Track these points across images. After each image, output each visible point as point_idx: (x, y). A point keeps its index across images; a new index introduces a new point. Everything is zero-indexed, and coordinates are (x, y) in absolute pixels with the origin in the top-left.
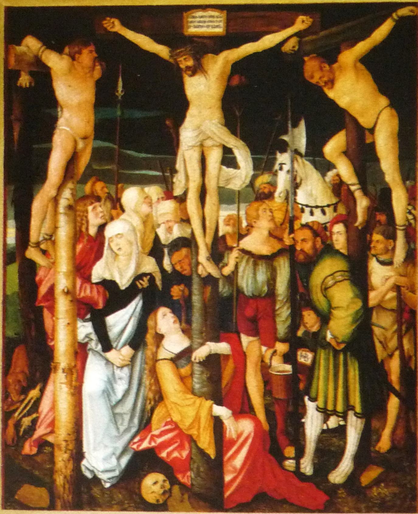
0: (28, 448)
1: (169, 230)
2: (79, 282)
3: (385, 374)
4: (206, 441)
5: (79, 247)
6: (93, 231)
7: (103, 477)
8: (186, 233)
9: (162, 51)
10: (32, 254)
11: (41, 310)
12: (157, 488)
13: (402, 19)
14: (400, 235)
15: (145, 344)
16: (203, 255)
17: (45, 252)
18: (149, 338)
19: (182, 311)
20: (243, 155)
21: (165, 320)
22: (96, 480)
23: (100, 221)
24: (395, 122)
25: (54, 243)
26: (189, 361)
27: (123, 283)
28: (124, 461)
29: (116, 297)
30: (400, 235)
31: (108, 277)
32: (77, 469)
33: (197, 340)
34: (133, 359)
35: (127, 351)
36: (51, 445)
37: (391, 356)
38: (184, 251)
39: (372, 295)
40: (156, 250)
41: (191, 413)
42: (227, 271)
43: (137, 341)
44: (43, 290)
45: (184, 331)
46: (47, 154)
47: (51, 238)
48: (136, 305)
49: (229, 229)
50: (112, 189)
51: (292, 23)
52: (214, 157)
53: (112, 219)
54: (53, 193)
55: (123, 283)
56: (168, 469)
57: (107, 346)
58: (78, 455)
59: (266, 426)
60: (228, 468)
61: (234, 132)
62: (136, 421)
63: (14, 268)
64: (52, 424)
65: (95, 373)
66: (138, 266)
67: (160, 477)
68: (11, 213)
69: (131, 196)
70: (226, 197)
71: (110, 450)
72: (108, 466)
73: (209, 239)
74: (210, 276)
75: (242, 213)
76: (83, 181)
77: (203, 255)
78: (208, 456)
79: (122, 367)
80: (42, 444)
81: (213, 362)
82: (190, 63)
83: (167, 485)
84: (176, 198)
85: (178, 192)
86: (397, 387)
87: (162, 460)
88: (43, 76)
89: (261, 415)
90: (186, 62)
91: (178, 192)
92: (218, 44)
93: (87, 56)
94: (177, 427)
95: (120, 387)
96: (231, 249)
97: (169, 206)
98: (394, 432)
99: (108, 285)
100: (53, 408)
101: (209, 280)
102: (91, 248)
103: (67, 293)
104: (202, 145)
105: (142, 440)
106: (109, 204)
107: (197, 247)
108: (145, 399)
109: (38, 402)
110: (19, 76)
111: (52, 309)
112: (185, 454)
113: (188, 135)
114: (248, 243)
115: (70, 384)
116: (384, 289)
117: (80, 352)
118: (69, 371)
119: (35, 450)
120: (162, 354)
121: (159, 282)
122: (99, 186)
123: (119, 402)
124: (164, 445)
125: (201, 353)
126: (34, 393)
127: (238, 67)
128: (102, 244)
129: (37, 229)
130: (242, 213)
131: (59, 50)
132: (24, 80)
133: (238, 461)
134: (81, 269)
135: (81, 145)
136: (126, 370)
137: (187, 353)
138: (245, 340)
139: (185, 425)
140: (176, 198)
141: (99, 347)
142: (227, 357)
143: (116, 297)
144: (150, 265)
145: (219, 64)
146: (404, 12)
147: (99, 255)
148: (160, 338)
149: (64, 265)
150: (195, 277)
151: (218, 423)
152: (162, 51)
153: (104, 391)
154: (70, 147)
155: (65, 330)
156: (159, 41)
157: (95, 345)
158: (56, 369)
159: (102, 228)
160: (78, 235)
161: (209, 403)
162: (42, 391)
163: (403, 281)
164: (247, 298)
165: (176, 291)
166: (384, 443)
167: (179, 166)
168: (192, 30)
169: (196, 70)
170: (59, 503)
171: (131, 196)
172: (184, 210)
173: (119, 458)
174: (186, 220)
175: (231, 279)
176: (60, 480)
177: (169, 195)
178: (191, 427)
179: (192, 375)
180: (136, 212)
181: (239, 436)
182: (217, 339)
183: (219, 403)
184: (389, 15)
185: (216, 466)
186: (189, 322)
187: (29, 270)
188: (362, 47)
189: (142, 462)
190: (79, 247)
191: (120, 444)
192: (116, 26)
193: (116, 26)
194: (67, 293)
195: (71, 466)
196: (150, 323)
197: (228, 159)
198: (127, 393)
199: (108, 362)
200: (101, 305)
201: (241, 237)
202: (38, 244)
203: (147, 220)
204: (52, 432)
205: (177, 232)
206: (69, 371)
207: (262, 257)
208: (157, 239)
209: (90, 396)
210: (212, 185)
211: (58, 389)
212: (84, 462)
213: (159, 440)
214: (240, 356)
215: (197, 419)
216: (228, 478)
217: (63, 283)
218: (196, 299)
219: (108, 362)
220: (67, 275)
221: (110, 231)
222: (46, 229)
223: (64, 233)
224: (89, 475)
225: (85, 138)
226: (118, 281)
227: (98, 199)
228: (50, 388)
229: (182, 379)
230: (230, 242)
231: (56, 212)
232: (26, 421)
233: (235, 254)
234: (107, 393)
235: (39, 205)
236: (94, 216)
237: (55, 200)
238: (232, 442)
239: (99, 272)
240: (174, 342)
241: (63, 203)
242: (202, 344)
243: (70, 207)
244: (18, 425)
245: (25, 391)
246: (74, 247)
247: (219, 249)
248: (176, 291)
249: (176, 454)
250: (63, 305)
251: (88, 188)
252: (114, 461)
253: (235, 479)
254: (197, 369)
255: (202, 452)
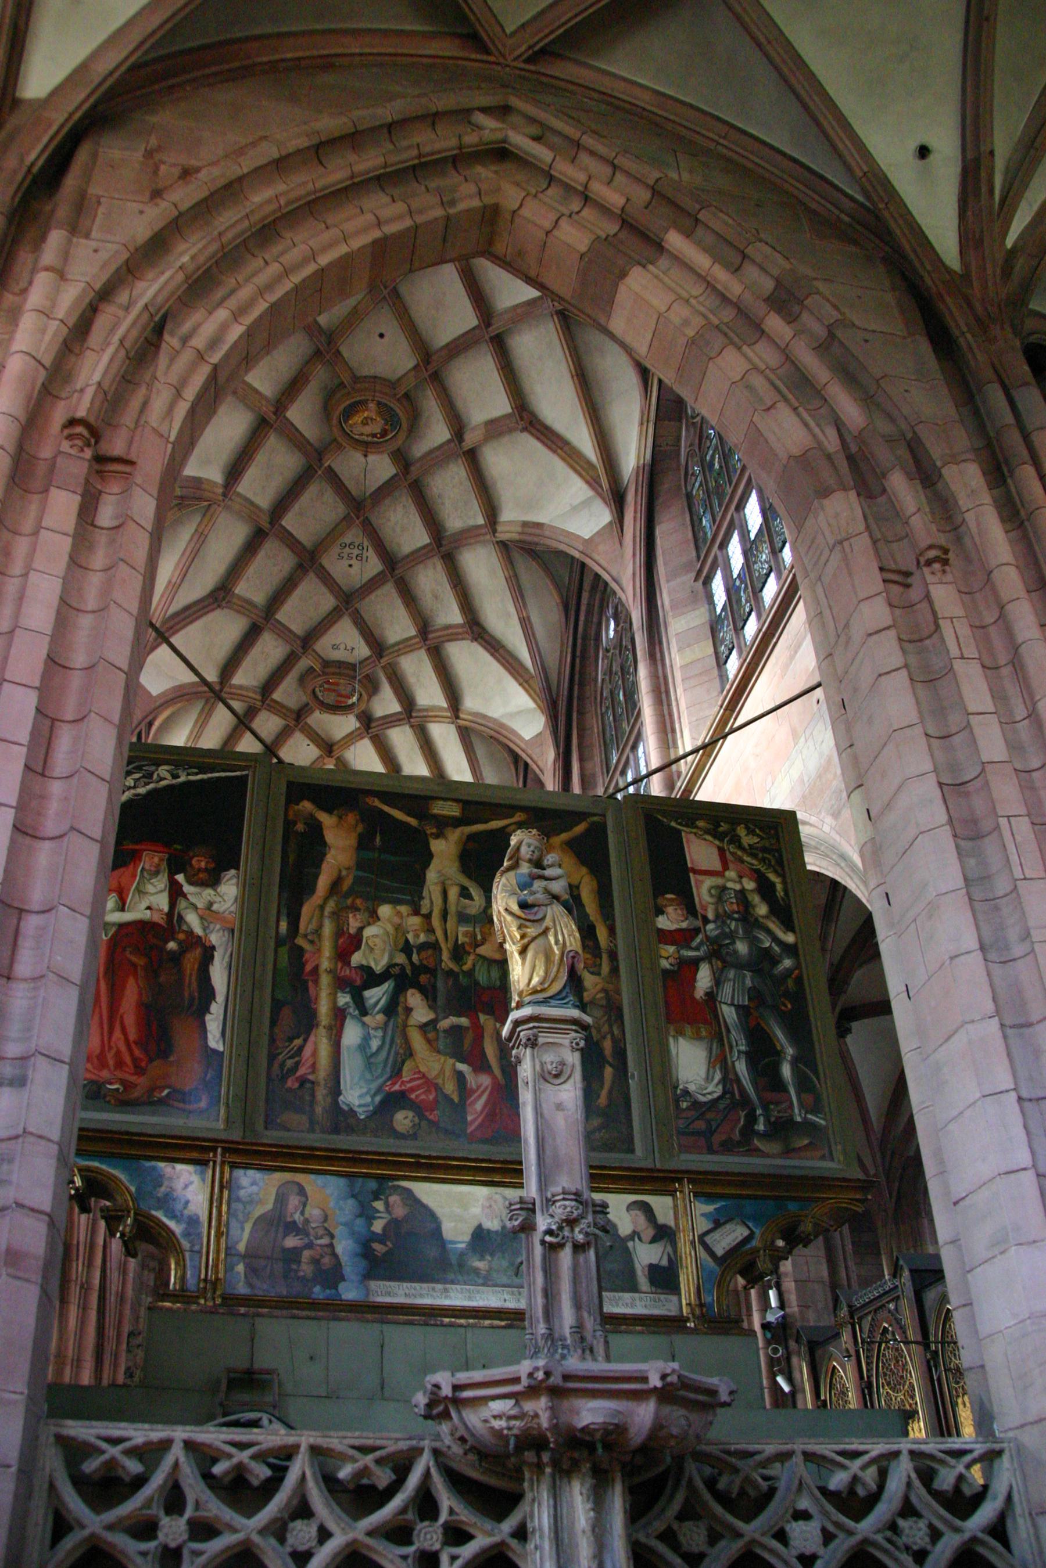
0: (291, 1083)
1: (417, 936)
2: (340, 965)
3: (601, 1051)
4: (450, 1088)
5: (341, 941)
6: (352, 931)
7: (359, 1110)
8: (432, 939)
9: (413, 822)
10: (300, 941)
11: (306, 982)
12: (407, 1122)
13: (593, 823)
14: (605, 956)
15: (397, 1014)
16: (445, 956)
17: (312, 942)
18: (400, 1009)
19: (429, 994)
20: (475, 891)
21: (414, 998)
22: (352, 1112)
23: (358, 924)
24: (595, 883)
25: (320, 936)
26: (435, 1029)
27: (378, 968)
28: (378, 1099)
29: (372, 979)
30: (605, 956)
31: (364, 963)
32: (336, 1102)
33: (441, 1015)
34: (386, 1024)
35: (380, 1018)
36: (313, 1083)
37: (604, 1038)
38: (430, 952)
39: (585, 994)
40: (407, 949)
41: (437, 1067)
42: (465, 968)
43: (391, 1009)
44: (308, 968)
45: (430, 1007)
46: (316, 876)
47: (318, 932)
48: (387, 986)
49: (467, 940)
50: (370, 904)
51: (512, 816)
52: (453, 893)
53: (369, 924)
54: (320, 902)
55: (378, 968)
56: (419, 1109)
57: (364, 1012)
58: (336, 1090)
59: (502, 1081)
60: (469, 1109)
61: (470, 877)
62: (388, 1069)
63: (284, 951)
64: (314, 1067)
65: (352, 1034)
66: (391, 957)
67: (411, 1114)
68: (284, 911)
69: (385, 910)
70: (463, 918)
71: (365, 1090)
72: (363, 1102)
73: (451, 944)
74: (451, 970)
75: (477, 930)
76: (346, 896)
77: (445, 956)
78: (452, 1100)
79: (376, 1029)
80: (303, 1081)
81: (456, 1029)
82: (434, 830)
83: (417, 1120)
84: (424, 916)
85: (424, 911)
86: (610, 1059)
87: (411, 1100)
88: (316, 830)
89: (497, 1071)
90: (431, 830)
91: (424, 911)
92: (457, 822)
93: (351, 818)
94: (424, 1076)
95: (375, 1044)
96: (469, 953)
97: (415, 921)
98: (610, 1092)
99: (367, 970)
100: (315, 1053)
101: (450, 973)
102: (349, 944)
103: (330, 972)
104: (443, 883)
105: (394, 1084)
106: (366, 914)
107: (441, 950)
108: (397, 1053)
109: (301, 1049)
110: (295, 823)
111: (316, 982)
112: (431, 1097)
113: (432, 875)
114: (482, 950)
115: (330, 1039)
116: (594, 991)
117: (339, 1015)
118: (329, 1028)
119: (296, 1085)
120: (412, 1021)
121: (408, 972)
122: (358, 902)
123: (373, 1055)
124: (412, 1090)
125: (445, 1024)
126: (298, 1042)
127: (471, 837)
128: (360, 941)
129: (305, 924)
130: (477, 930)
131: (329, 811)
132: (300, 827)
133: (479, 1106)
134: (343, 955)
135: (344, 873)
136: (380, 1033)
137: (433, 1023)
138: (482, 1018)
139: (432, 1075)
140: (424, 916)
141: (357, 1012)
142: (467, 1028)
143: (372, 979)
144: (401, 959)
145: (455, 835)
146: (595, 819)
147: (358, 947)
148: (409, 1010)
149: (327, 950)
150: (439, 972)
151: (460, 1076)
152: (413, 822)
153: (360, 1046)
154: (335, 874)
155: (325, 1000)
156: (409, 815)
157: (353, 1010)
158: (317, 1025)
159: (361, 929)
160: (340, 932)
161: (451, 1061)
162: (305, 1040)
163: (610, 987)
164: (483, 988)
165: (423, 979)
166: (603, 1100)
167: (425, 893)
168: (435, 811)
169: (437, 836)
170: (317, 1127)
171: (385, 910)
172: (429, 923)
173: (373, 1097)
174: (431, 930)
175: (470, 973)
176: (319, 1110)
177: (416, 912)
178: (436, 1077)
179: (437, 1039)
180: (389, 921)
181: (479, 1087)
182: (460, 1015)
183: (463, 1061)
184: (585, 820)
185: (460, 1108)
186: (435, 1000)
187: (298, 953)
188: (564, 836)
189: (391, 1102)
190: (341, 941)
191: (374, 1086)
192: (377, 803)
193: (377, 803)
194: (330, 972)
195: (329, 1100)
196: (402, 999)
197: (465, 893)
198: (380, 1048)
199: (364, 1024)
200: (359, 982)
201: (477, 946)
202: (305, 936)
203: (398, 928)
204: (313, 1072)
205: (422, 938)
206: (329, 1028)
207: (495, 961)
208: (407, 941)
209: (348, 1048)
210: (452, 909)
211: (320, 1043)
212: (341, 1098)
213: (409, 1085)
214: (479, 1032)
215: (442, 1071)
216: (469, 1118)
217: (325, 964)
218: (440, 984)
219: (364, 1024)
220: (330, 959)
221: (368, 932)
222: (313, 926)
223: (328, 929)
224: (346, 1108)
225: (348, 869)
226: (373, 965)
227: (358, 909)
228: (312, 1038)
229: (429, 1041)
230: (467, 948)
231: (322, 915)
232: (290, 1063)
233: (472, 957)
234: (363, 1046)
235: (306, 910)
236: (353, 923)
237: (322, 908)
238: (474, 1091)
239: (357, 959)
240: (421, 1013)
241: (328, 910)
242: (446, 1018)
243: (334, 913)
244: (282, 1065)
245: (291, 1039)
246: (336, 941)
247: (458, 953)
248: (423, 979)
249: (423, 1097)
250: (325, 980)
251: (349, 901)
252: (368, 1099)
253: (475, 1119)
254: (441, 1035)
255: (446, 1097)
